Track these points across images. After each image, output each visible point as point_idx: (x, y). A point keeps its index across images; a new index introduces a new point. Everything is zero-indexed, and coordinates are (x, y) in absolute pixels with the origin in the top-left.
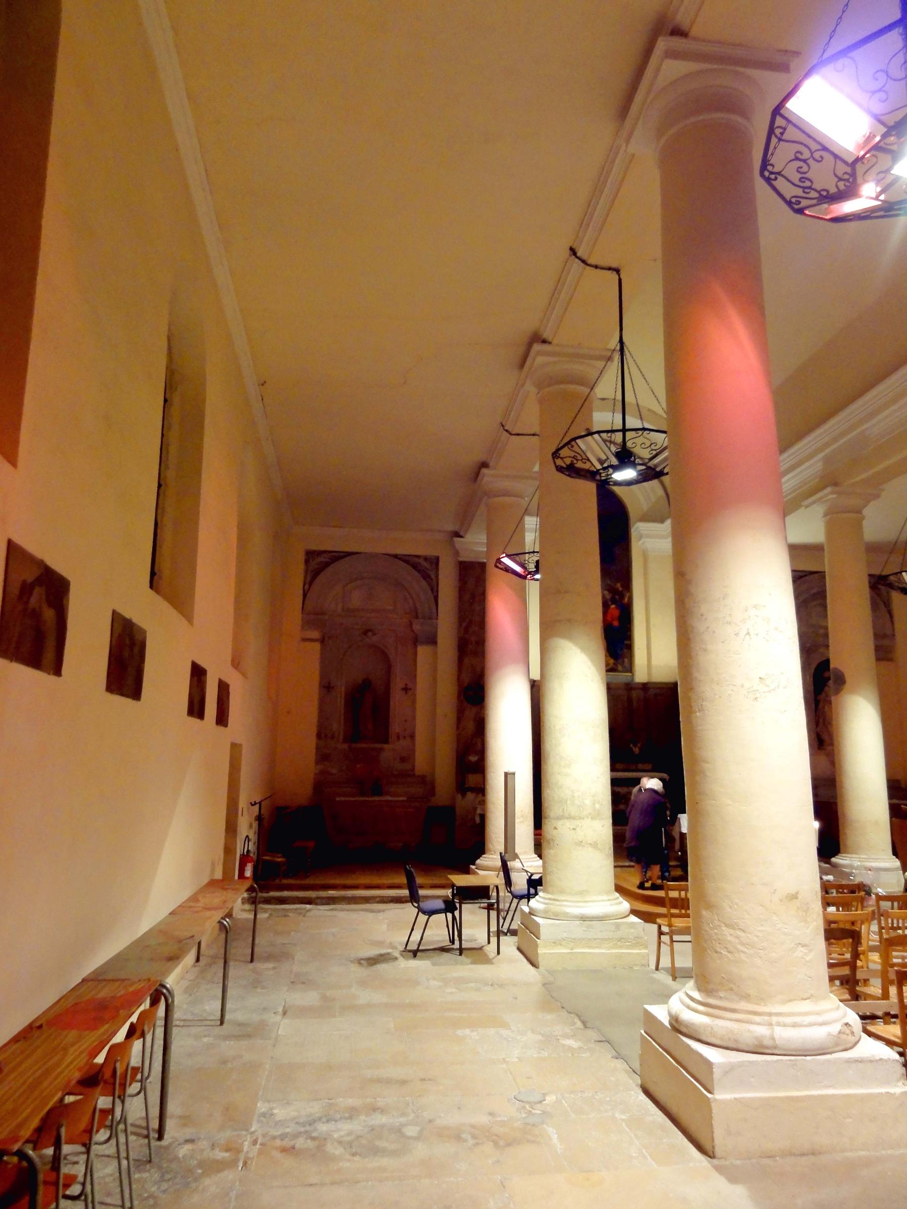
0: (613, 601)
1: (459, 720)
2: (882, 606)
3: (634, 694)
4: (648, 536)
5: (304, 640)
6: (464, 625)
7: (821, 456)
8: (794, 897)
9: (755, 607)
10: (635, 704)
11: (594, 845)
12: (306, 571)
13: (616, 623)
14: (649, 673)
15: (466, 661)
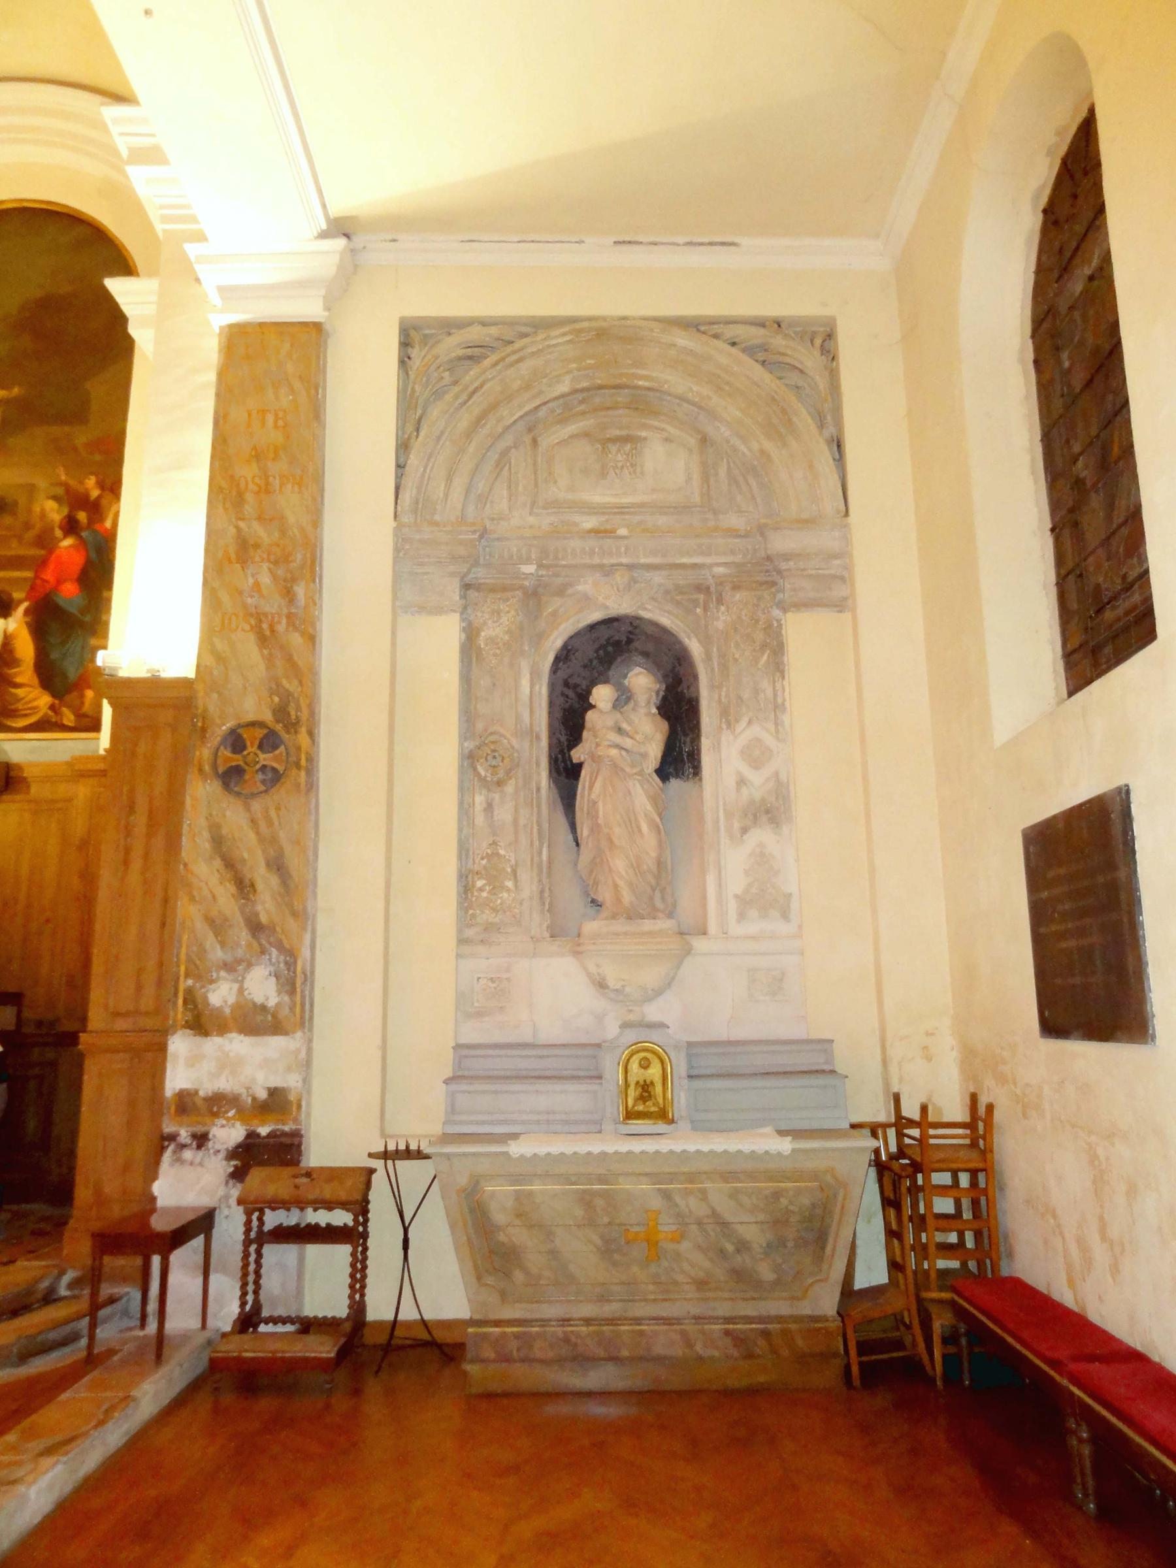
0: (71, 526)
2: (804, 420)
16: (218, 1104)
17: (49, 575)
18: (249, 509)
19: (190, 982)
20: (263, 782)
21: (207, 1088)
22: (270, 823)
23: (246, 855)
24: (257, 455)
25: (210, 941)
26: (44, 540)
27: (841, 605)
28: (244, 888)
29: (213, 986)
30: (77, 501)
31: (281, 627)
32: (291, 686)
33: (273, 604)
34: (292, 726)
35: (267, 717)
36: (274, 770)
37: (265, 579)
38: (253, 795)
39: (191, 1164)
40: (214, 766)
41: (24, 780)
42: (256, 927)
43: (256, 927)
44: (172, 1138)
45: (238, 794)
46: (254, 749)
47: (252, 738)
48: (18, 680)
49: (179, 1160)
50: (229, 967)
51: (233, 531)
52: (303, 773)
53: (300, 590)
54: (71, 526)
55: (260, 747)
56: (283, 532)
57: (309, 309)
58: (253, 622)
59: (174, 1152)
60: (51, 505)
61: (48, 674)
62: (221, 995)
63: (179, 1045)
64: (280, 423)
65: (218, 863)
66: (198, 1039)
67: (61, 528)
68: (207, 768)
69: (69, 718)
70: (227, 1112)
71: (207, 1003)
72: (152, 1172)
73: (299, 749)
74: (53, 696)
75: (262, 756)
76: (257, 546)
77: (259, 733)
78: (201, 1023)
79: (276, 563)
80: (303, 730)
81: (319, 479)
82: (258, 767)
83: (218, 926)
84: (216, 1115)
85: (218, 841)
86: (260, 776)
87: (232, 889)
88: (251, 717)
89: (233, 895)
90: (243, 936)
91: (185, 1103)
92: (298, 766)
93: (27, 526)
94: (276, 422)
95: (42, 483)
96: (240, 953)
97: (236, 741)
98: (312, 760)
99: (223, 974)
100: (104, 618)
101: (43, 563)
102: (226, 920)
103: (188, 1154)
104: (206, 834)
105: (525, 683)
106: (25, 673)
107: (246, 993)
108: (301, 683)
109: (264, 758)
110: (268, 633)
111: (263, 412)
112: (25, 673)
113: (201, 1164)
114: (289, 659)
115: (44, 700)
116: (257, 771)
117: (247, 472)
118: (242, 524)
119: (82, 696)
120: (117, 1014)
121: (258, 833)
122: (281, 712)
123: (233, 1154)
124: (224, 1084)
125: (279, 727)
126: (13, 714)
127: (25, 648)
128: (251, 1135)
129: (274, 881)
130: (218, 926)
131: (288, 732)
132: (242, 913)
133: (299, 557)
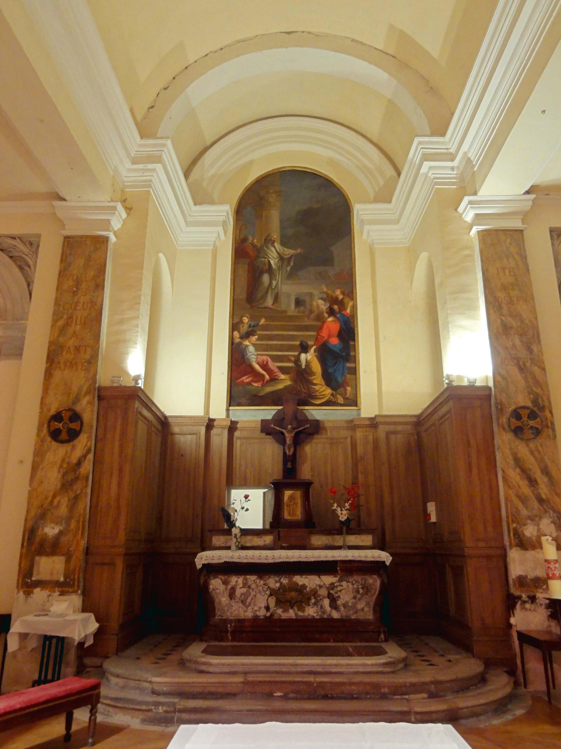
0: (331, 312)
1: (35, 468)
3: (359, 434)
6: (60, 323)
10: (360, 450)
13: (334, 342)
14: (380, 406)
15: (58, 375)
17: (324, 333)
18: (505, 311)
19: (514, 525)
20: (533, 433)
21: (531, 575)
22: (539, 453)
23: (531, 467)
24: (504, 288)
25: (520, 506)
26: (320, 318)
28: (532, 482)
29: (525, 527)
30: (334, 301)
31: (528, 364)
32: (538, 391)
33: (523, 353)
34: (542, 409)
35: (529, 404)
36: (537, 428)
37: (518, 342)
38: (529, 440)
39: (530, 610)
40: (509, 426)
41: (325, 429)
42: (541, 501)
43: (541, 501)
44: (519, 598)
45: (522, 439)
46: (526, 419)
47: (524, 413)
48: (315, 382)
49: (523, 608)
50: (532, 518)
51: (499, 321)
52: (550, 430)
53: (535, 348)
54: (331, 312)
55: (529, 418)
56: (522, 321)
57: (517, 224)
58: (515, 361)
59: (521, 604)
60: (321, 302)
61: (329, 379)
64: (512, 274)
65: (518, 470)
66: (523, 552)
67: (327, 313)
68: (506, 426)
69: (341, 400)
70: (542, 586)
71: (524, 535)
73: (546, 419)
74: (332, 389)
75: (530, 422)
76: (511, 328)
77: (527, 412)
79: (521, 335)
80: (547, 410)
81: (533, 298)
82: (529, 427)
83: (524, 500)
84: (537, 587)
85: (518, 461)
86: (531, 431)
87: (526, 482)
88: (522, 404)
89: (527, 485)
90: (536, 504)
91: (522, 581)
92: (548, 427)
93: (311, 312)
94: (510, 273)
95: (316, 292)
96: (535, 512)
97: (516, 414)
98: (552, 423)
99: (529, 521)
100: (352, 354)
101: (321, 328)
102: (526, 497)
103: (528, 606)
104: (511, 457)
107: (541, 530)
108: (542, 389)
109: (532, 423)
110: (522, 366)
111: (504, 269)
113: (534, 610)
114: (534, 378)
115: (329, 391)
116: (529, 429)
117: (501, 295)
118: (503, 318)
119: (346, 390)
120: (479, 540)
121: (535, 457)
122: (535, 402)
125: (535, 409)
126: (315, 398)
127: (317, 367)
129: (546, 479)
130: (524, 500)
131: (540, 411)
132: (533, 493)
133: (531, 333)
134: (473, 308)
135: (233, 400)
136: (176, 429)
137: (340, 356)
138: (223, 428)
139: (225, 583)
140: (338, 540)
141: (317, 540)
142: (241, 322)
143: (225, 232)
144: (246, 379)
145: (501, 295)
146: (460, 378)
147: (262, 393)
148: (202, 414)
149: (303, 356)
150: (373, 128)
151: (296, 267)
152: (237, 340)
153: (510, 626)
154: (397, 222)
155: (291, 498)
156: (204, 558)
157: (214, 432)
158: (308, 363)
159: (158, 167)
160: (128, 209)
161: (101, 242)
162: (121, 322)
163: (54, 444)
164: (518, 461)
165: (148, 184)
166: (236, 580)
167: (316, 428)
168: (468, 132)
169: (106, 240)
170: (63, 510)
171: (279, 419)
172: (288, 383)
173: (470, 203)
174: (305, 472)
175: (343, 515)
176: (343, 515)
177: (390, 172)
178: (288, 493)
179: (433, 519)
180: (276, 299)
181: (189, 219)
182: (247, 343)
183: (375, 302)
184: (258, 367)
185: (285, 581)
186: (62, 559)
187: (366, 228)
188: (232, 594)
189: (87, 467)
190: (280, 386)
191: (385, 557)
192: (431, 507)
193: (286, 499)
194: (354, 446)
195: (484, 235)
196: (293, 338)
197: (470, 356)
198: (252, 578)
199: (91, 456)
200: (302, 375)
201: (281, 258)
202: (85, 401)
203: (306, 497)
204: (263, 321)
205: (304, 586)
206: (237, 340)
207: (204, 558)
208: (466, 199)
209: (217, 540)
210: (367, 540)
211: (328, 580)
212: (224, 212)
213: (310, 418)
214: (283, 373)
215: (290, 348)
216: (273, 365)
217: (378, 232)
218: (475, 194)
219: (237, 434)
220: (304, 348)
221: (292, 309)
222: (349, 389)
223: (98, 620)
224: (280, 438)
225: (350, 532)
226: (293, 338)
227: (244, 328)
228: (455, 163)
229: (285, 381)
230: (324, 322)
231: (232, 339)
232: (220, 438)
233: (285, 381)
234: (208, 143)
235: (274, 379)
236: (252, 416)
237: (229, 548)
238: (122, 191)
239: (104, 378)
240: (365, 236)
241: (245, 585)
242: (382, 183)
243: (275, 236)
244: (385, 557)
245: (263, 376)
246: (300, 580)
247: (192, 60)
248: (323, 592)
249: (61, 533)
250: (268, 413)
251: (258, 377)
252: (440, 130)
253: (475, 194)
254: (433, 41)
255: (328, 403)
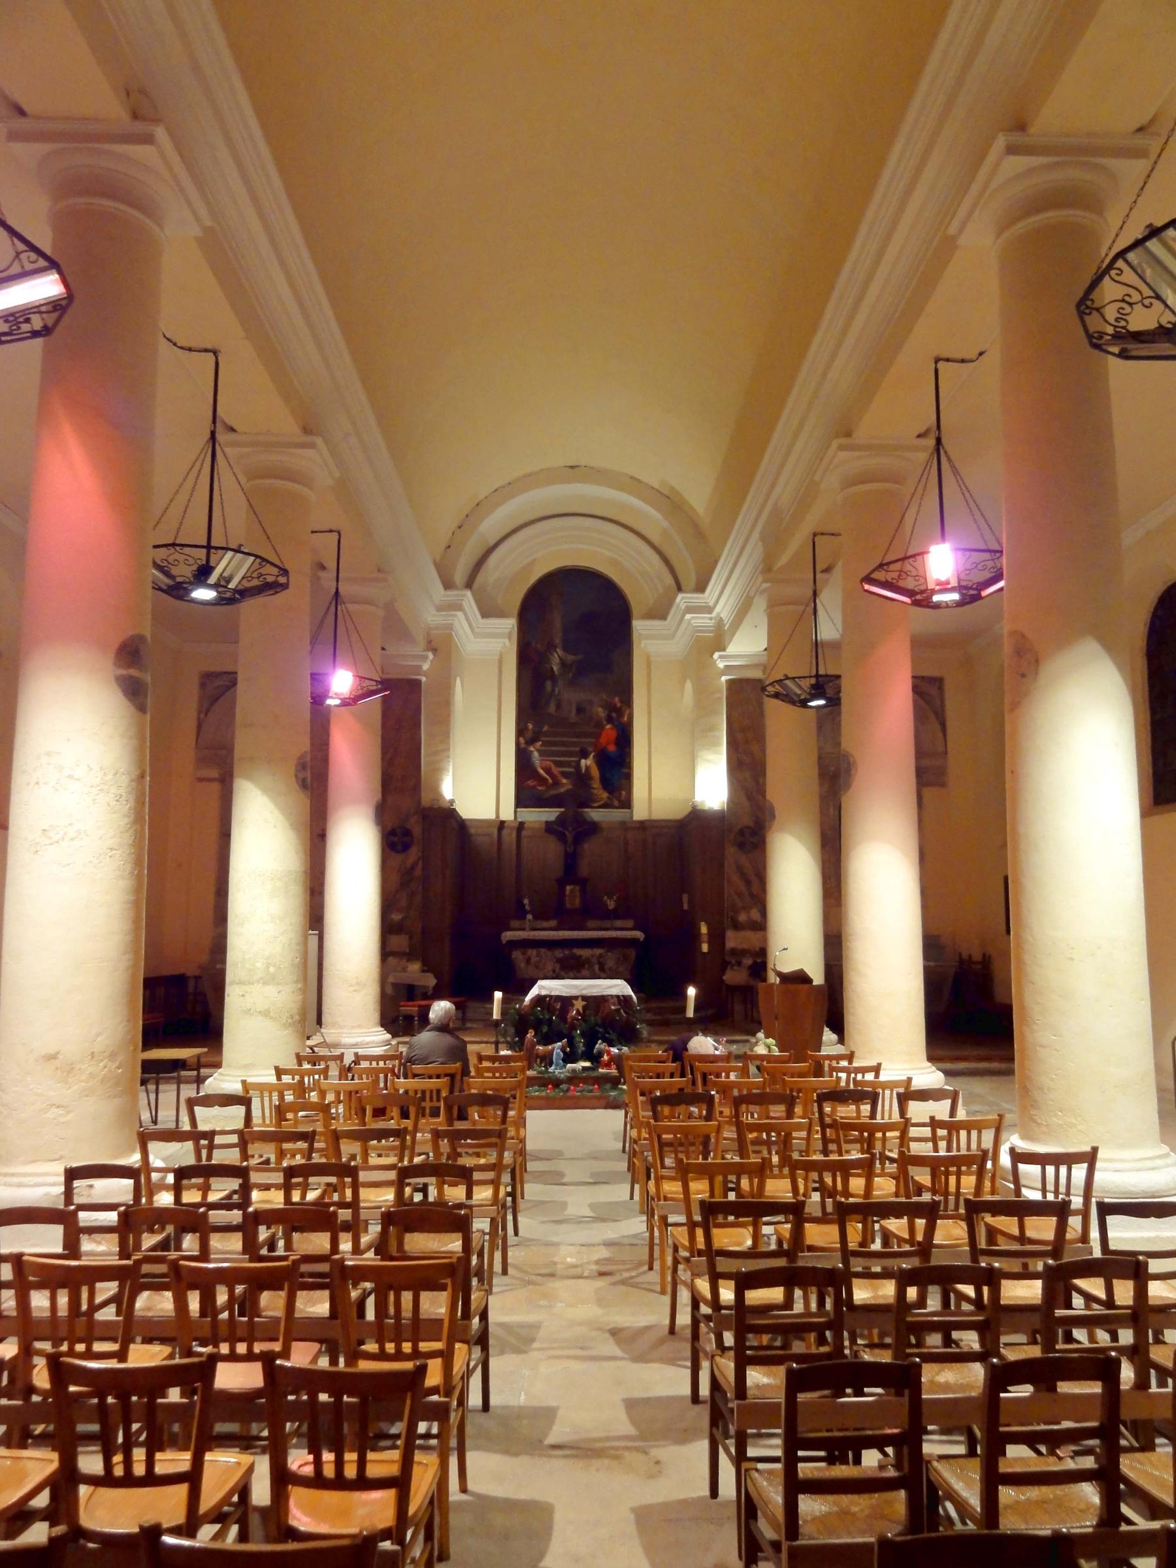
0: (610, 720)
2: (933, 718)
4: (648, 637)
5: (200, 780)
7: (756, 535)
8: (52, 1057)
9: (48, 754)
11: (266, 1014)
12: (201, 699)
13: (612, 748)
16: (744, 952)
17: (603, 740)
21: (740, 947)
26: (599, 725)
27: (943, 785)
28: (748, 883)
35: (752, 824)
42: (752, 895)
43: (752, 895)
49: (732, 968)
60: (600, 710)
61: (606, 784)
62: (742, 917)
63: (730, 934)
69: (616, 803)
72: (724, 974)
74: (610, 792)
78: (737, 926)
83: (740, 895)
85: (740, 869)
91: (734, 952)
97: (741, 832)
105: (831, 810)
106: (596, 784)
112: (596, 784)
115: (605, 795)
117: (739, 736)
123: (750, 967)
124: (746, 946)
127: (595, 772)
128: (755, 963)
130: (740, 895)
134: (719, 744)
135: (520, 802)
136: (472, 831)
137: (617, 765)
138: (511, 828)
139: (524, 954)
140: (607, 923)
141: (591, 923)
142: (526, 728)
143: (510, 640)
144: (531, 783)
145: (739, 736)
146: (703, 802)
147: (547, 795)
148: (493, 816)
149: (583, 762)
150: (655, 538)
151: (578, 672)
152: (523, 746)
153: (723, 981)
154: (673, 636)
155: (572, 891)
156: (508, 936)
157: (505, 832)
158: (587, 768)
159: (460, 614)
160: (435, 650)
161: (417, 684)
162: (435, 753)
163: (393, 854)
164: (740, 869)
165: (450, 627)
166: (532, 953)
167: (593, 828)
168: (721, 598)
169: (419, 682)
170: (403, 903)
171: (561, 820)
172: (570, 787)
173: (720, 657)
174: (584, 869)
175: (611, 905)
176: (611, 905)
177: (669, 580)
178: (568, 888)
179: (686, 907)
180: (558, 706)
181: (476, 630)
182: (532, 749)
183: (649, 713)
184: (541, 772)
185: (567, 952)
186: (407, 937)
187: (643, 643)
188: (528, 961)
189: (418, 872)
190: (562, 790)
191: (639, 935)
192: (685, 898)
193: (567, 892)
194: (626, 843)
195: (730, 683)
196: (574, 744)
197: (711, 787)
198: (543, 950)
199: (420, 864)
200: (582, 779)
201: (563, 664)
202: (413, 820)
203: (583, 891)
204: (546, 728)
205: (580, 956)
206: (523, 746)
207: (508, 936)
208: (716, 655)
209: (515, 923)
210: (630, 923)
211: (598, 951)
212: (510, 624)
213: (588, 819)
214: (566, 778)
215: (571, 754)
216: (556, 770)
217: (653, 644)
218: (724, 650)
219: (524, 833)
220: (585, 755)
221: (573, 716)
222: (624, 793)
223: (436, 977)
224: (561, 837)
225: (618, 917)
226: (574, 744)
227: (529, 735)
228: (714, 615)
229: (566, 784)
230: (603, 728)
231: (518, 744)
232: (510, 837)
233: (566, 784)
234: (492, 542)
235: (556, 783)
236: (537, 816)
237: (523, 929)
238: (428, 634)
239: (426, 799)
240: (643, 645)
241: (538, 955)
242: (661, 591)
243: (558, 640)
244: (639, 935)
245: (546, 780)
246: (579, 952)
247: (482, 497)
248: (594, 960)
249: (403, 919)
250: (550, 814)
251: (542, 780)
252: (701, 588)
253: (724, 650)
254: (699, 496)
255: (605, 806)
